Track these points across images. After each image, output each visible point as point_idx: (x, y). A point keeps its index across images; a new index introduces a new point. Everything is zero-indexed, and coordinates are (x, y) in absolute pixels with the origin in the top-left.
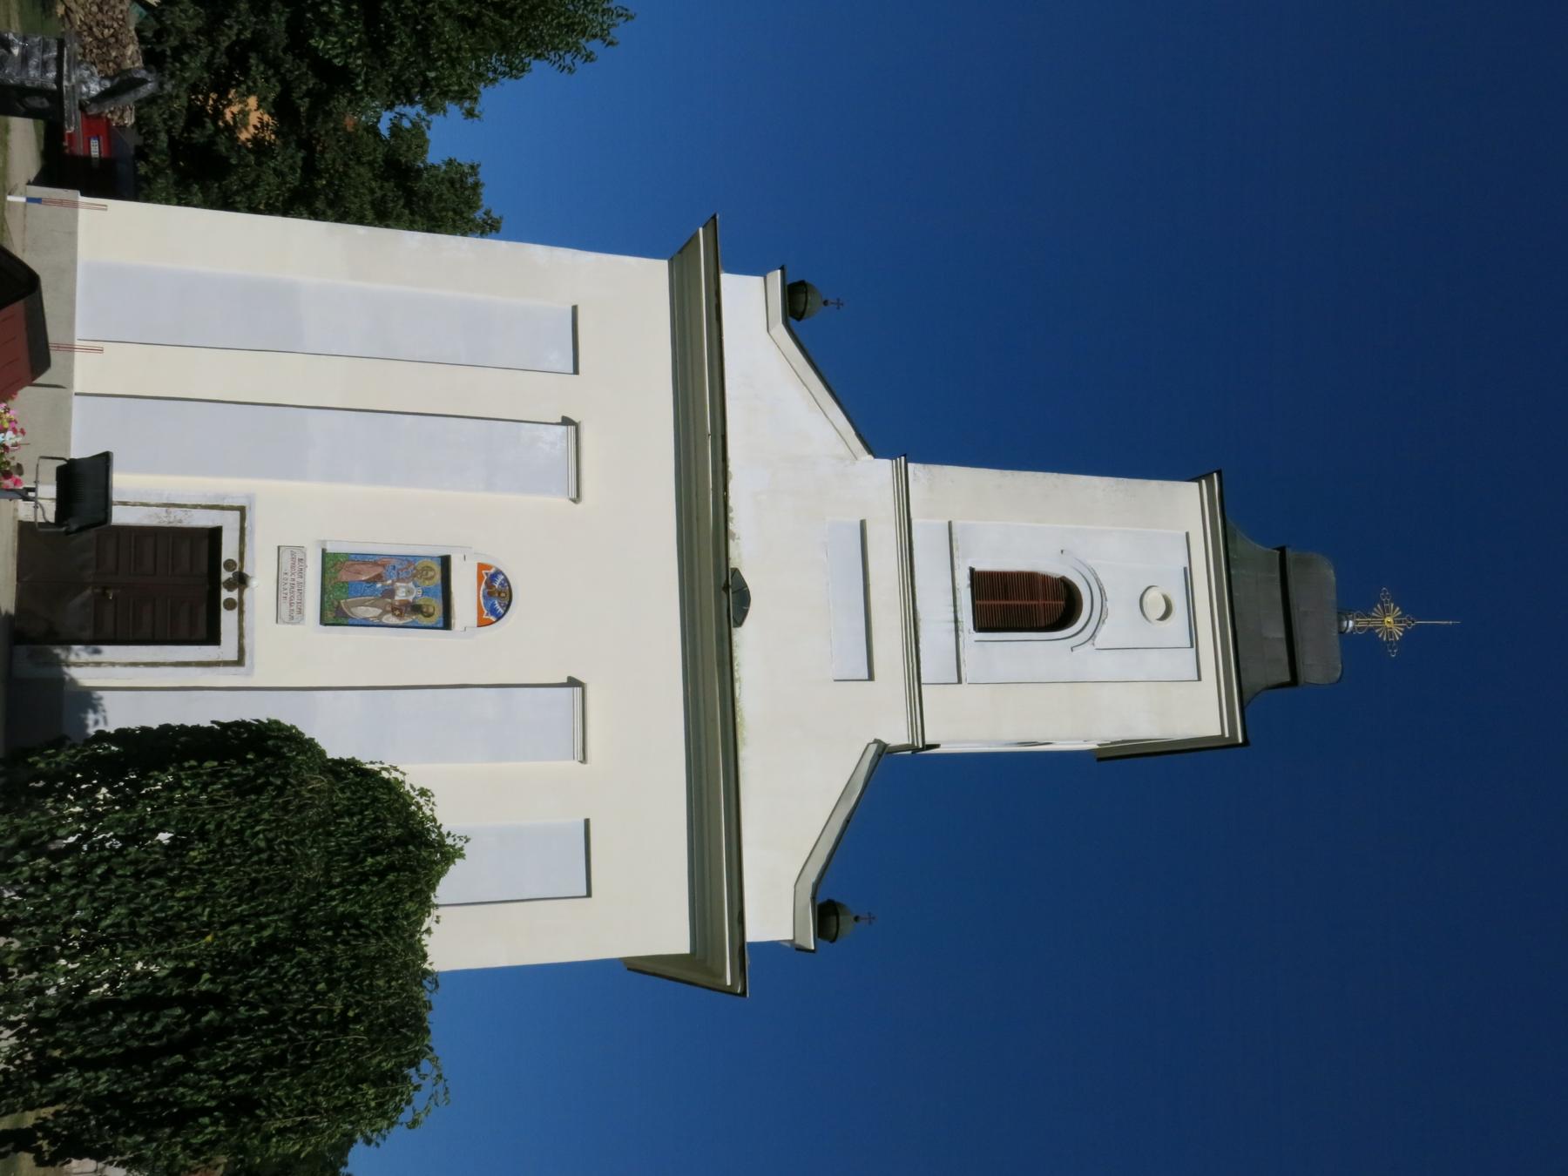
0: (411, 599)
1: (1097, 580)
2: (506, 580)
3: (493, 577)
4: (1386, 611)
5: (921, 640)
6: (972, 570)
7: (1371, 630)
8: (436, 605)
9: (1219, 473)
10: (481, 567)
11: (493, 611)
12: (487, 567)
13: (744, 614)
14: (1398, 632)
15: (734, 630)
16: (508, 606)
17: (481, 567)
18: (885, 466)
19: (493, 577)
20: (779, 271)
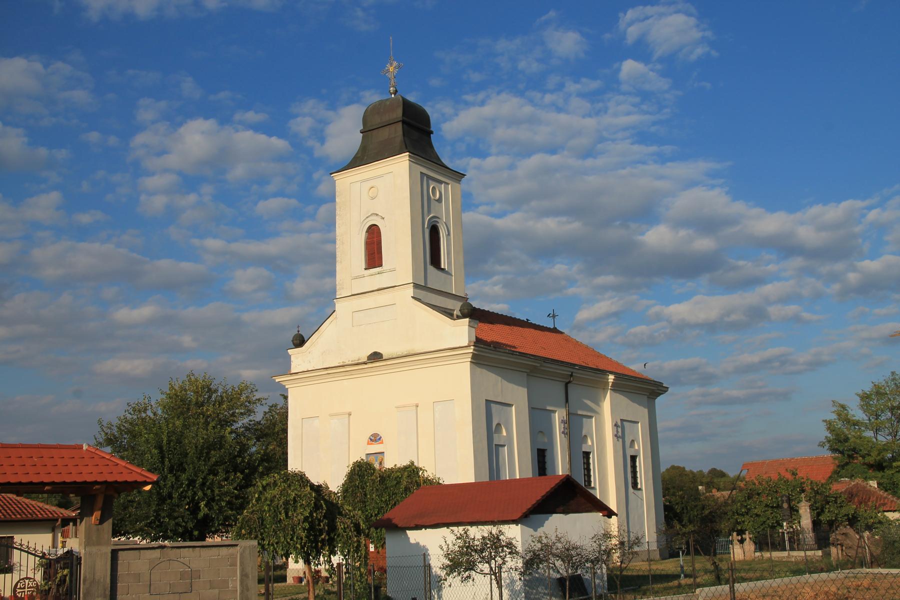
0: (378, 465)
1: (365, 219)
2: (372, 435)
3: (371, 440)
4: (388, 71)
5: (385, 286)
6: (365, 269)
7: (395, 77)
8: (380, 456)
9: (331, 174)
10: (368, 444)
11: (380, 439)
12: (368, 441)
13: (379, 353)
14: (395, 64)
15: (384, 358)
16: (378, 435)
17: (368, 444)
18: (340, 306)
19: (371, 440)
20: (289, 350)
